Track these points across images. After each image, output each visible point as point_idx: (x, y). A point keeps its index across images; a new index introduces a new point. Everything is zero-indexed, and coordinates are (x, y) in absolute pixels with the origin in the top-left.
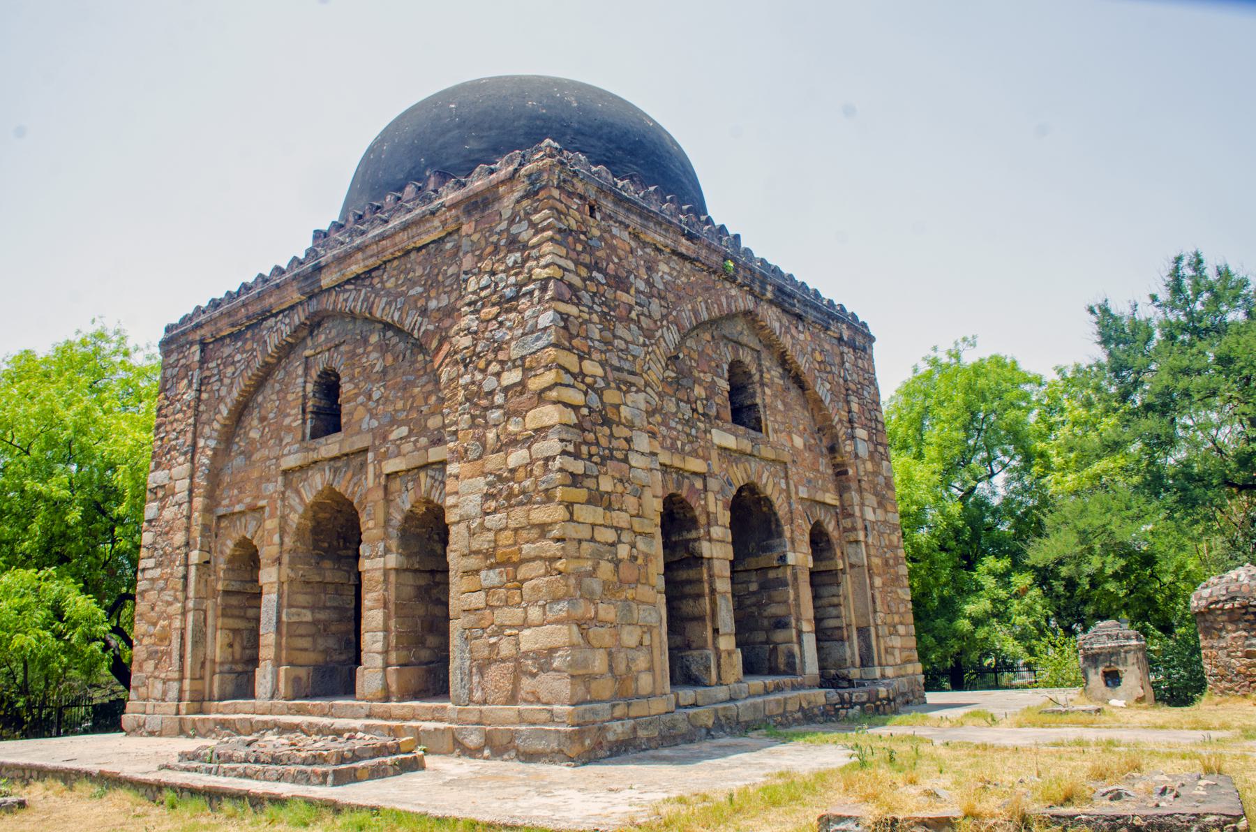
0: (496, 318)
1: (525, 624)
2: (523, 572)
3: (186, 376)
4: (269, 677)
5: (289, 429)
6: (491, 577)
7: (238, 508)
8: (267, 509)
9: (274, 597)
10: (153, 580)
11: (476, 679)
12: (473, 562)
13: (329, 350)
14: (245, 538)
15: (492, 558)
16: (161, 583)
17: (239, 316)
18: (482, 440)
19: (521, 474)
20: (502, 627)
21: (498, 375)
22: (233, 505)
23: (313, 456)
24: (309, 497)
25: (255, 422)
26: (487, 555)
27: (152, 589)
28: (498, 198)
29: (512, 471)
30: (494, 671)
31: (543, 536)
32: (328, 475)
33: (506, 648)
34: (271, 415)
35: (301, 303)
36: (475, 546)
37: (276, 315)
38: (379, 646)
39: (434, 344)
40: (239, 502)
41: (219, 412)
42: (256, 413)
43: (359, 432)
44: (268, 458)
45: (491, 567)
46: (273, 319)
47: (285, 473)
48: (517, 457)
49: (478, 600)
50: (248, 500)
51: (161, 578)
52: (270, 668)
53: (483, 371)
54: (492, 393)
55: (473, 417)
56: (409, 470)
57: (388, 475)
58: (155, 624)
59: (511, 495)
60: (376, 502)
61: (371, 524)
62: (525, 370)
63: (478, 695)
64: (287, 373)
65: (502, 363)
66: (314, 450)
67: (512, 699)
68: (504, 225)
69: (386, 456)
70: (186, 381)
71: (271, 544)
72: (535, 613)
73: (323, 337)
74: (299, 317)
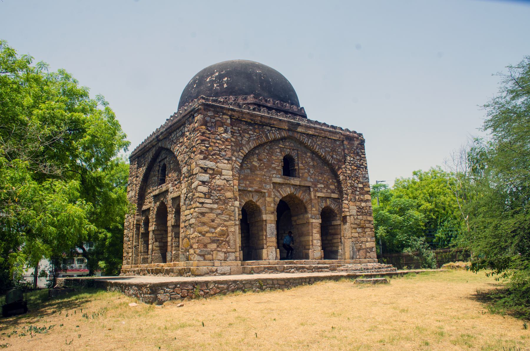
1: (367, 242)
2: (366, 230)
3: (222, 126)
4: (274, 252)
5: (274, 168)
6: (360, 230)
7: (250, 189)
8: (267, 194)
10: (212, 209)
11: (357, 253)
12: (355, 226)
15: (360, 226)
16: (219, 211)
17: (256, 118)
18: (355, 199)
19: (365, 208)
20: (362, 242)
21: (358, 184)
22: (247, 187)
23: (287, 182)
24: (284, 195)
25: (256, 160)
26: (358, 225)
27: (211, 212)
28: (354, 141)
29: (363, 207)
30: (361, 251)
31: (369, 223)
32: (293, 190)
33: (363, 247)
34: (265, 160)
35: (285, 130)
36: (356, 222)
37: (272, 127)
38: (319, 244)
39: (337, 168)
40: (250, 187)
41: (243, 149)
43: (307, 181)
44: (265, 175)
45: (359, 228)
46: (270, 128)
47: (274, 183)
48: (363, 204)
49: (357, 235)
50: (256, 188)
51: (219, 209)
52: (274, 249)
53: (354, 181)
54: (356, 187)
58: (215, 228)
59: (363, 213)
60: (315, 204)
61: (314, 209)
62: (364, 185)
63: (358, 257)
64: (271, 148)
67: (365, 258)
68: (355, 148)
69: (317, 191)
70: (222, 129)
71: (270, 206)
72: (369, 239)
73: (288, 144)
74: (284, 134)
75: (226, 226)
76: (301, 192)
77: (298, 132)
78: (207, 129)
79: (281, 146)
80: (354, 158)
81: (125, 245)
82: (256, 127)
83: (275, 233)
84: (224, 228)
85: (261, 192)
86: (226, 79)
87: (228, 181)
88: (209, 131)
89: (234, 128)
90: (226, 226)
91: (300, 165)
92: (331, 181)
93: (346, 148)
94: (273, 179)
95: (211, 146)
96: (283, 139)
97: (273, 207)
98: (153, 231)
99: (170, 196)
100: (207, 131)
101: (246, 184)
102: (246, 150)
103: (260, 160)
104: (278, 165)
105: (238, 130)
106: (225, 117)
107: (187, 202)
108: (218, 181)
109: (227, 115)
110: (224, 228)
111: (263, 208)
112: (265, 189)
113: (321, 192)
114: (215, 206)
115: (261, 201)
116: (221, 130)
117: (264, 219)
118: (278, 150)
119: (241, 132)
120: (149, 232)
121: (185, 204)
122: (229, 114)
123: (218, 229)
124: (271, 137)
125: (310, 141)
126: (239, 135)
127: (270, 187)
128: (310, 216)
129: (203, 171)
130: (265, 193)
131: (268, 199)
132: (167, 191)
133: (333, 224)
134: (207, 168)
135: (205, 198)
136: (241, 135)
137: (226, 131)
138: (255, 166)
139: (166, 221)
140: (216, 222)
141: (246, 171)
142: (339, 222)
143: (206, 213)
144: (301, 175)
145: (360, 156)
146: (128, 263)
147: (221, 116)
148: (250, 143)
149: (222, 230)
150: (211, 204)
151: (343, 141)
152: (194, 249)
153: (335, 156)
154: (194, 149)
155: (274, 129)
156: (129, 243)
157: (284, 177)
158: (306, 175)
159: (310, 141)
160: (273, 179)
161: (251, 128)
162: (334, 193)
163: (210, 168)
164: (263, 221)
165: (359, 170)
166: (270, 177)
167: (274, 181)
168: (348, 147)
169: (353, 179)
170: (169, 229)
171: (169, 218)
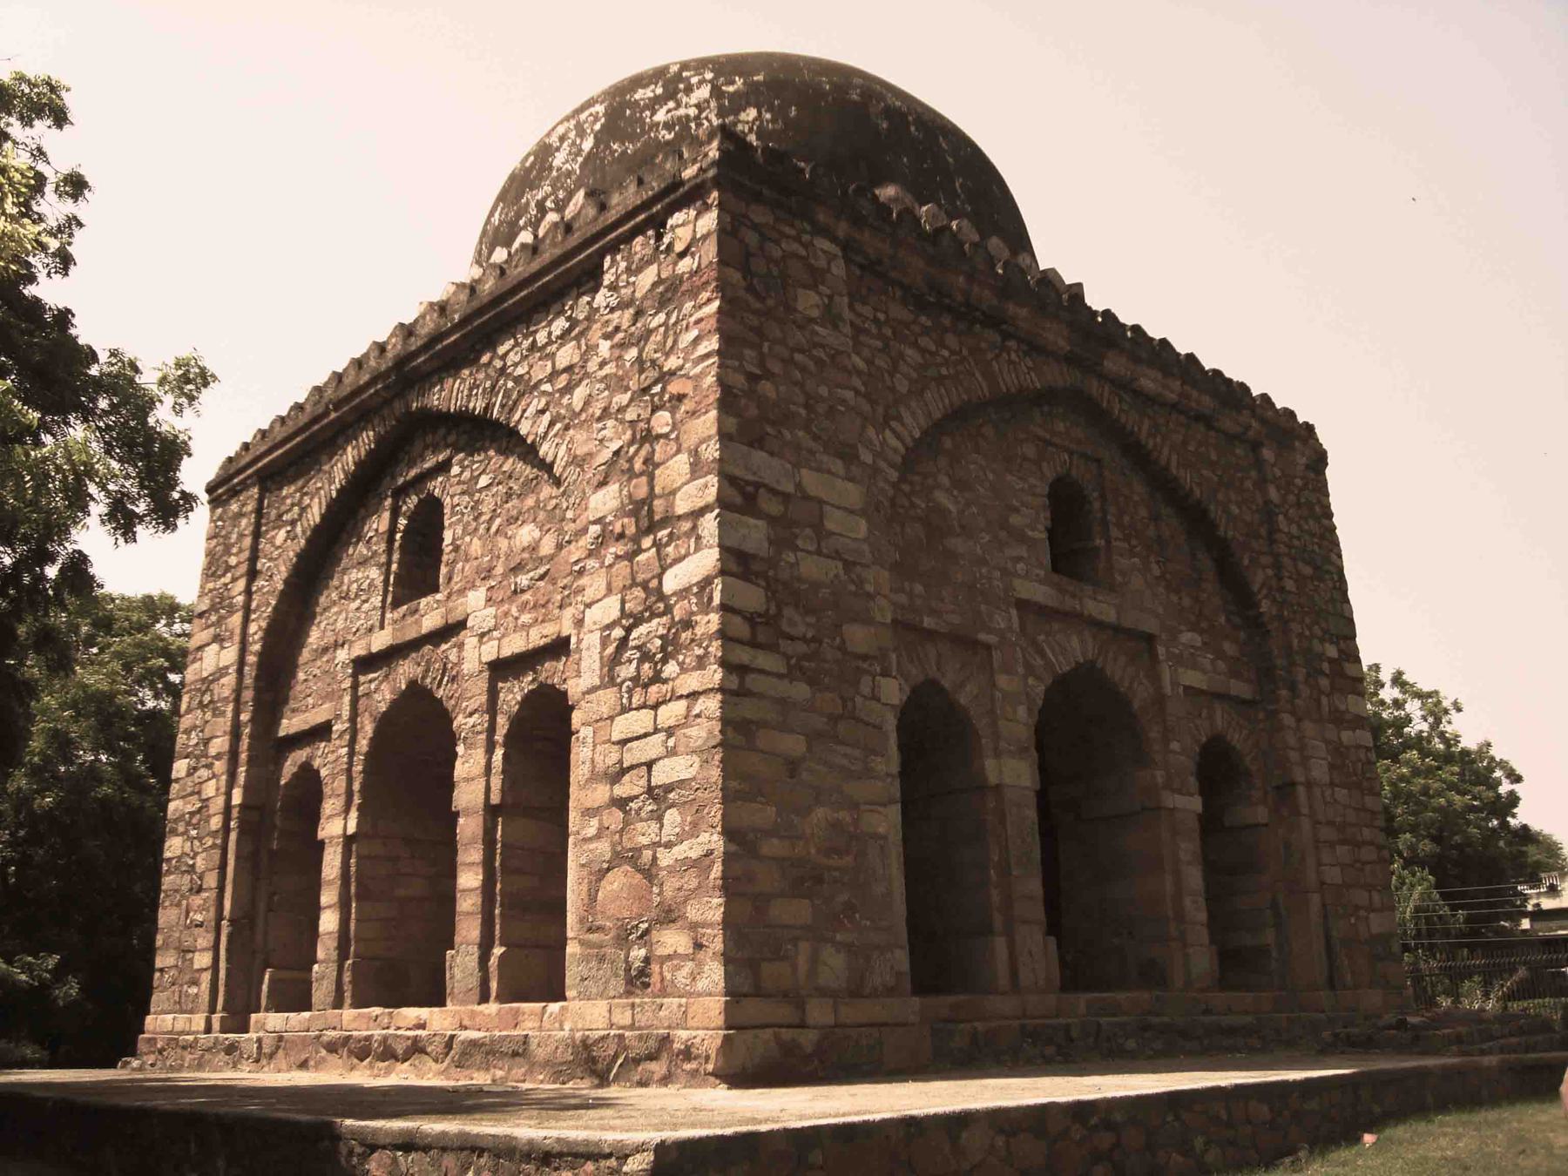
0: (1312, 578)
3: (814, 287)
5: (1022, 538)
7: (928, 622)
8: (997, 656)
9: (1031, 814)
13: (1071, 453)
14: (932, 685)
16: (819, 722)
23: (1070, 604)
25: (945, 481)
29: (1347, 748)
37: (1006, 336)
39: (1246, 562)
40: (933, 612)
41: (899, 418)
42: (943, 462)
44: (982, 562)
45: (1343, 842)
46: (999, 339)
47: (1023, 605)
50: (955, 619)
52: (1038, 935)
53: (1310, 629)
55: (1308, 675)
56: (1201, 692)
57: (1186, 688)
65: (1325, 632)
66: (1074, 596)
69: (1178, 660)
70: (813, 298)
73: (1061, 427)
75: (854, 806)
76: (1122, 660)
77: (1102, 377)
78: (750, 289)
79: (1040, 432)
80: (1299, 526)
81: (167, 916)
82: (946, 321)
83: (1037, 854)
84: (844, 816)
85: (976, 644)
86: (752, 113)
87: (848, 566)
88: (761, 299)
89: (858, 307)
90: (854, 806)
91: (1115, 532)
92: (1222, 620)
93: (1270, 477)
94: (1017, 583)
95: (768, 375)
96: (1045, 398)
97: (1019, 722)
98: (348, 840)
99: (473, 655)
100: (751, 299)
101: (911, 595)
102: (913, 423)
103: (960, 484)
104: (1033, 520)
105: (876, 320)
106: (823, 244)
107: (626, 671)
108: (813, 568)
109: (834, 239)
110: (844, 816)
111: (981, 724)
112: (990, 631)
113: (1195, 666)
114: (800, 691)
115: (971, 688)
116: (808, 302)
117: (993, 779)
118: (1030, 450)
119: (889, 332)
120: (321, 846)
121: (610, 680)
122: (841, 234)
123: (820, 813)
124: (1009, 380)
125: (1145, 427)
126: (879, 344)
127: (1005, 620)
128: (1160, 776)
129: (738, 500)
130: (988, 647)
131: (1002, 680)
132: (451, 630)
133: (1227, 824)
134: (757, 485)
135: (753, 644)
136: (887, 346)
137: (830, 317)
138: (943, 512)
139: (447, 784)
140: (805, 775)
141: (908, 530)
142: (1261, 814)
143: (763, 724)
144: (1119, 578)
145: (1317, 519)
146: (180, 1007)
147: (805, 238)
148: (928, 395)
149: (836, 825)
150: (780, 676)
151: (1256, 446)
152: (694, 926)
153: (1235, 510)
154: (675, 387)
155: (1012, 344)
156: (197, 901)
157: (1056, 578)
158: (1137, 582)
159: (1145, 427)
160: (1017, 583)
161: (923, 319)
162: (1234, 674)
163: (765, 486)
164: (982, 788)
165: (1321, 580)
166: (1005, 572)
167: (1024, 595)
168: (1278, 473)
169: (1307, 620)
170: (469, 827)
171: (460, 770)
